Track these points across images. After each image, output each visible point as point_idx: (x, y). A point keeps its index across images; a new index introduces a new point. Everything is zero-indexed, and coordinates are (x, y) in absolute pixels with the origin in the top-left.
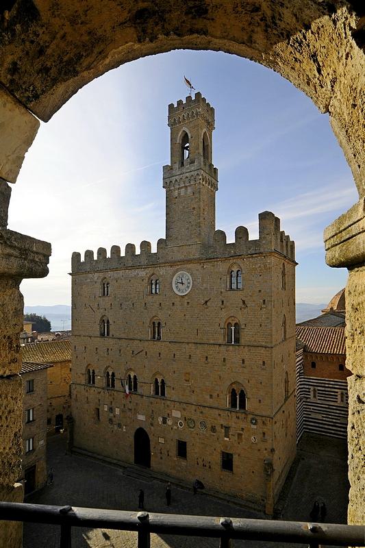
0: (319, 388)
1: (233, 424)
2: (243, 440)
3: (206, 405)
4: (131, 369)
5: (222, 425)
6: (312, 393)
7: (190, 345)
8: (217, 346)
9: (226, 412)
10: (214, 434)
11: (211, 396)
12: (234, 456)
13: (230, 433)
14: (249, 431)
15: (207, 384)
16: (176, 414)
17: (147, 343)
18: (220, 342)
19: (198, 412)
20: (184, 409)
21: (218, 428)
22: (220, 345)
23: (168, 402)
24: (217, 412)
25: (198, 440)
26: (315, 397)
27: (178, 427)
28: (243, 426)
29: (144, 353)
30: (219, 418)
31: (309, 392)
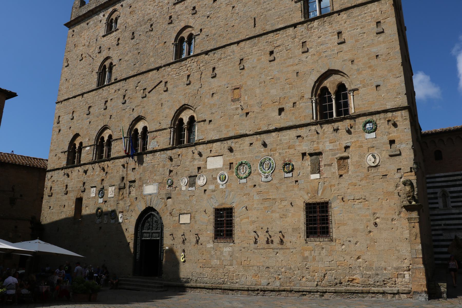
0: (452, 189)
1: (327, 144)
2: (351, 168)
3: (271, 128)
4: (139, 119)
5: (304, 154)
6: (440, 201)
7: (242, 44)
8: (291, 29)
9: (313, 128)
10: (290, 175)
11: (281, 110)
12: (333, 205)
13: (322, 164)
14: (361, 147)
15: (273, 92)
16: (214, 163)
17: (168, 69)
18: (295, 21)
19: (258, 144)
20: (231, 150)
21: (297, 162)
22: (295, 26)
23: (200, 148)
24: (293, 133)
25: (256, 197)
26: (445, 205)
27: (217, 186)
28: (346, 140)
29: (163, 83)
30: (297, 142)
31: (436, 198)
